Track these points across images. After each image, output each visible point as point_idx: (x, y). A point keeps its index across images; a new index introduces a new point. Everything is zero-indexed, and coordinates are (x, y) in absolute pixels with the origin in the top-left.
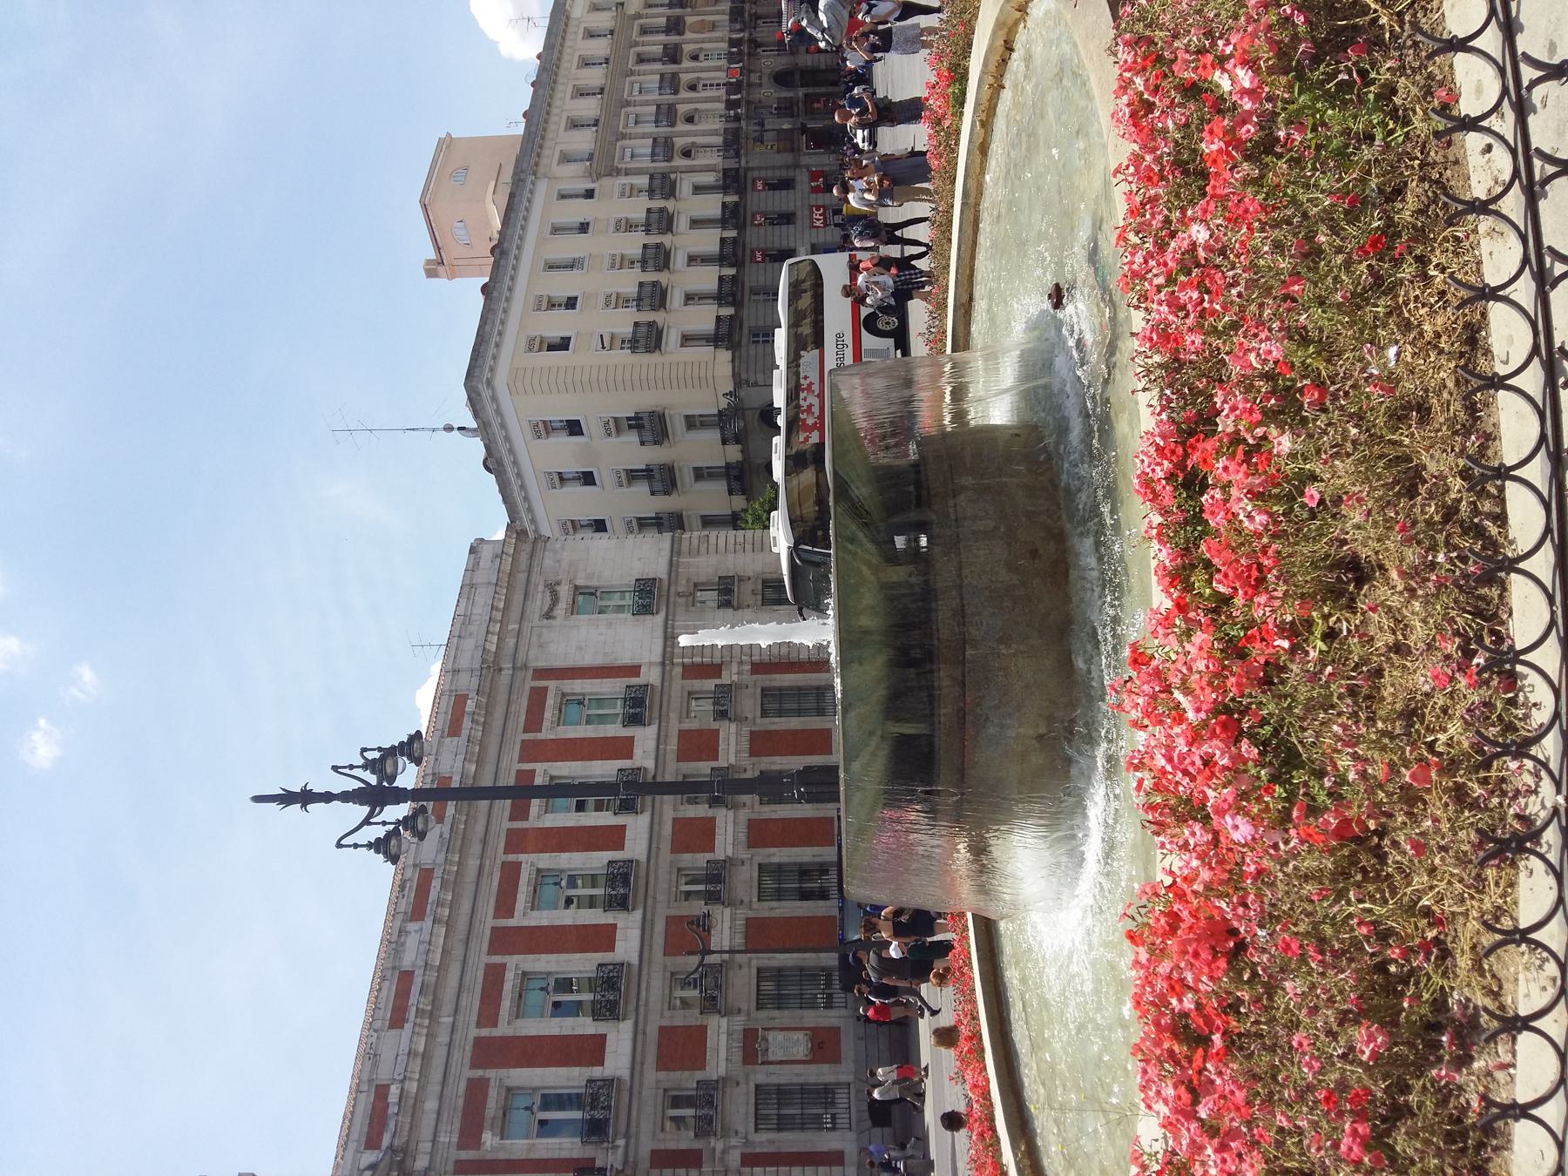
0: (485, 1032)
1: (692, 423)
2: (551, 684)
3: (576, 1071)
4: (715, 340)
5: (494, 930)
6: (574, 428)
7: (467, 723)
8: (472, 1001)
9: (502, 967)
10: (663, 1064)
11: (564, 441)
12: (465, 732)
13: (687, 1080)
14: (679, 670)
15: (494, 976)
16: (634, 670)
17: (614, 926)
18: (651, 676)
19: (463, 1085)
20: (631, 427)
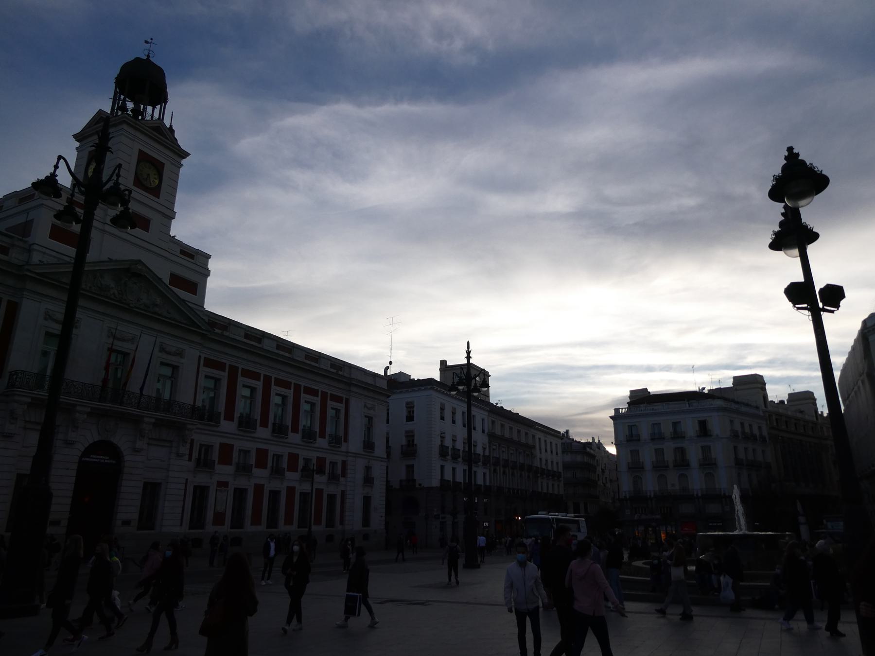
0: (240, 370)
1: (410, 468)
2: (343, 406)
3: (223, 408)
4: (442, 480)
5: (260, 374)
6: (410, 418)
7: (334, 371)
8: (251, 368)
9: (259, 380)
10: (222, 445)
11: (404, 413)
12: (332, 370)
13: (215, 455)
14: (344, 459)
15: (220, 366)
16: (346, 440)
17: (267, 427)
18: (344, 447)
19: (224, 361)
20: (409, 441)
